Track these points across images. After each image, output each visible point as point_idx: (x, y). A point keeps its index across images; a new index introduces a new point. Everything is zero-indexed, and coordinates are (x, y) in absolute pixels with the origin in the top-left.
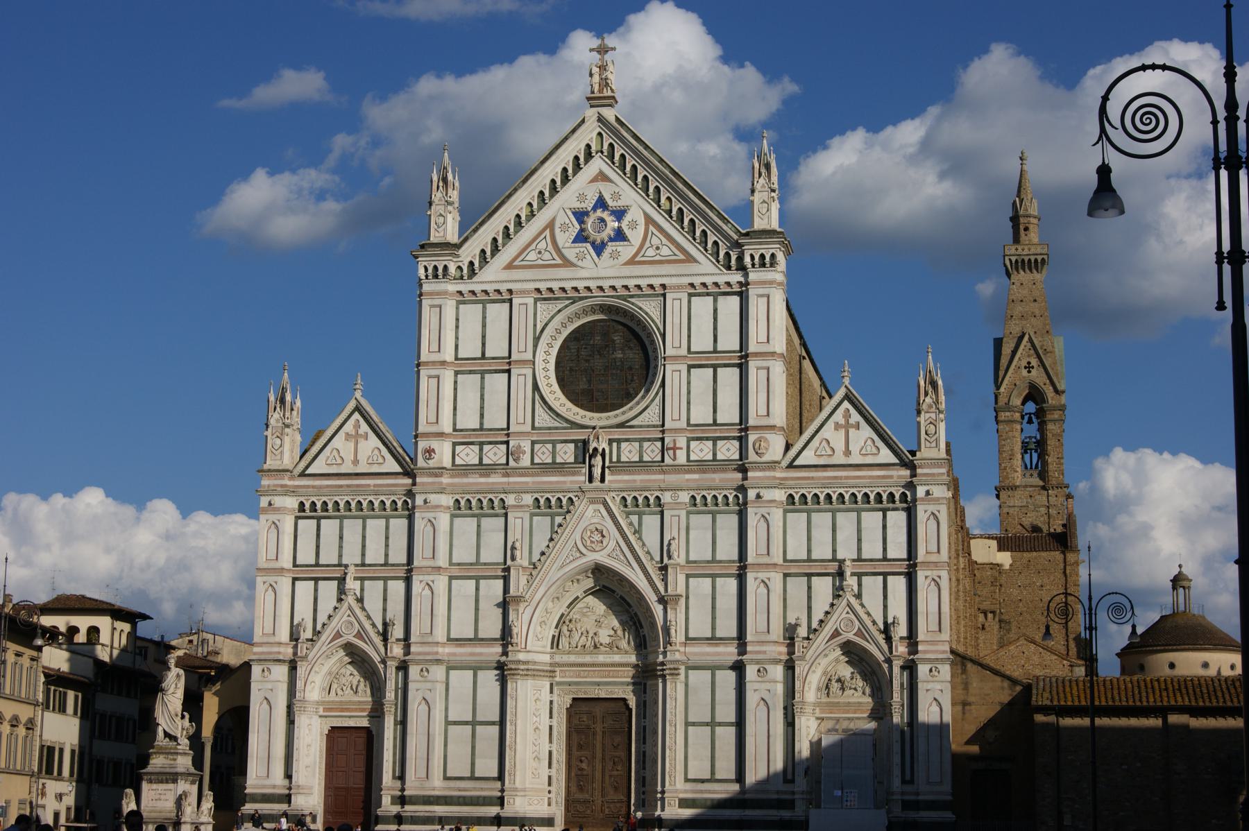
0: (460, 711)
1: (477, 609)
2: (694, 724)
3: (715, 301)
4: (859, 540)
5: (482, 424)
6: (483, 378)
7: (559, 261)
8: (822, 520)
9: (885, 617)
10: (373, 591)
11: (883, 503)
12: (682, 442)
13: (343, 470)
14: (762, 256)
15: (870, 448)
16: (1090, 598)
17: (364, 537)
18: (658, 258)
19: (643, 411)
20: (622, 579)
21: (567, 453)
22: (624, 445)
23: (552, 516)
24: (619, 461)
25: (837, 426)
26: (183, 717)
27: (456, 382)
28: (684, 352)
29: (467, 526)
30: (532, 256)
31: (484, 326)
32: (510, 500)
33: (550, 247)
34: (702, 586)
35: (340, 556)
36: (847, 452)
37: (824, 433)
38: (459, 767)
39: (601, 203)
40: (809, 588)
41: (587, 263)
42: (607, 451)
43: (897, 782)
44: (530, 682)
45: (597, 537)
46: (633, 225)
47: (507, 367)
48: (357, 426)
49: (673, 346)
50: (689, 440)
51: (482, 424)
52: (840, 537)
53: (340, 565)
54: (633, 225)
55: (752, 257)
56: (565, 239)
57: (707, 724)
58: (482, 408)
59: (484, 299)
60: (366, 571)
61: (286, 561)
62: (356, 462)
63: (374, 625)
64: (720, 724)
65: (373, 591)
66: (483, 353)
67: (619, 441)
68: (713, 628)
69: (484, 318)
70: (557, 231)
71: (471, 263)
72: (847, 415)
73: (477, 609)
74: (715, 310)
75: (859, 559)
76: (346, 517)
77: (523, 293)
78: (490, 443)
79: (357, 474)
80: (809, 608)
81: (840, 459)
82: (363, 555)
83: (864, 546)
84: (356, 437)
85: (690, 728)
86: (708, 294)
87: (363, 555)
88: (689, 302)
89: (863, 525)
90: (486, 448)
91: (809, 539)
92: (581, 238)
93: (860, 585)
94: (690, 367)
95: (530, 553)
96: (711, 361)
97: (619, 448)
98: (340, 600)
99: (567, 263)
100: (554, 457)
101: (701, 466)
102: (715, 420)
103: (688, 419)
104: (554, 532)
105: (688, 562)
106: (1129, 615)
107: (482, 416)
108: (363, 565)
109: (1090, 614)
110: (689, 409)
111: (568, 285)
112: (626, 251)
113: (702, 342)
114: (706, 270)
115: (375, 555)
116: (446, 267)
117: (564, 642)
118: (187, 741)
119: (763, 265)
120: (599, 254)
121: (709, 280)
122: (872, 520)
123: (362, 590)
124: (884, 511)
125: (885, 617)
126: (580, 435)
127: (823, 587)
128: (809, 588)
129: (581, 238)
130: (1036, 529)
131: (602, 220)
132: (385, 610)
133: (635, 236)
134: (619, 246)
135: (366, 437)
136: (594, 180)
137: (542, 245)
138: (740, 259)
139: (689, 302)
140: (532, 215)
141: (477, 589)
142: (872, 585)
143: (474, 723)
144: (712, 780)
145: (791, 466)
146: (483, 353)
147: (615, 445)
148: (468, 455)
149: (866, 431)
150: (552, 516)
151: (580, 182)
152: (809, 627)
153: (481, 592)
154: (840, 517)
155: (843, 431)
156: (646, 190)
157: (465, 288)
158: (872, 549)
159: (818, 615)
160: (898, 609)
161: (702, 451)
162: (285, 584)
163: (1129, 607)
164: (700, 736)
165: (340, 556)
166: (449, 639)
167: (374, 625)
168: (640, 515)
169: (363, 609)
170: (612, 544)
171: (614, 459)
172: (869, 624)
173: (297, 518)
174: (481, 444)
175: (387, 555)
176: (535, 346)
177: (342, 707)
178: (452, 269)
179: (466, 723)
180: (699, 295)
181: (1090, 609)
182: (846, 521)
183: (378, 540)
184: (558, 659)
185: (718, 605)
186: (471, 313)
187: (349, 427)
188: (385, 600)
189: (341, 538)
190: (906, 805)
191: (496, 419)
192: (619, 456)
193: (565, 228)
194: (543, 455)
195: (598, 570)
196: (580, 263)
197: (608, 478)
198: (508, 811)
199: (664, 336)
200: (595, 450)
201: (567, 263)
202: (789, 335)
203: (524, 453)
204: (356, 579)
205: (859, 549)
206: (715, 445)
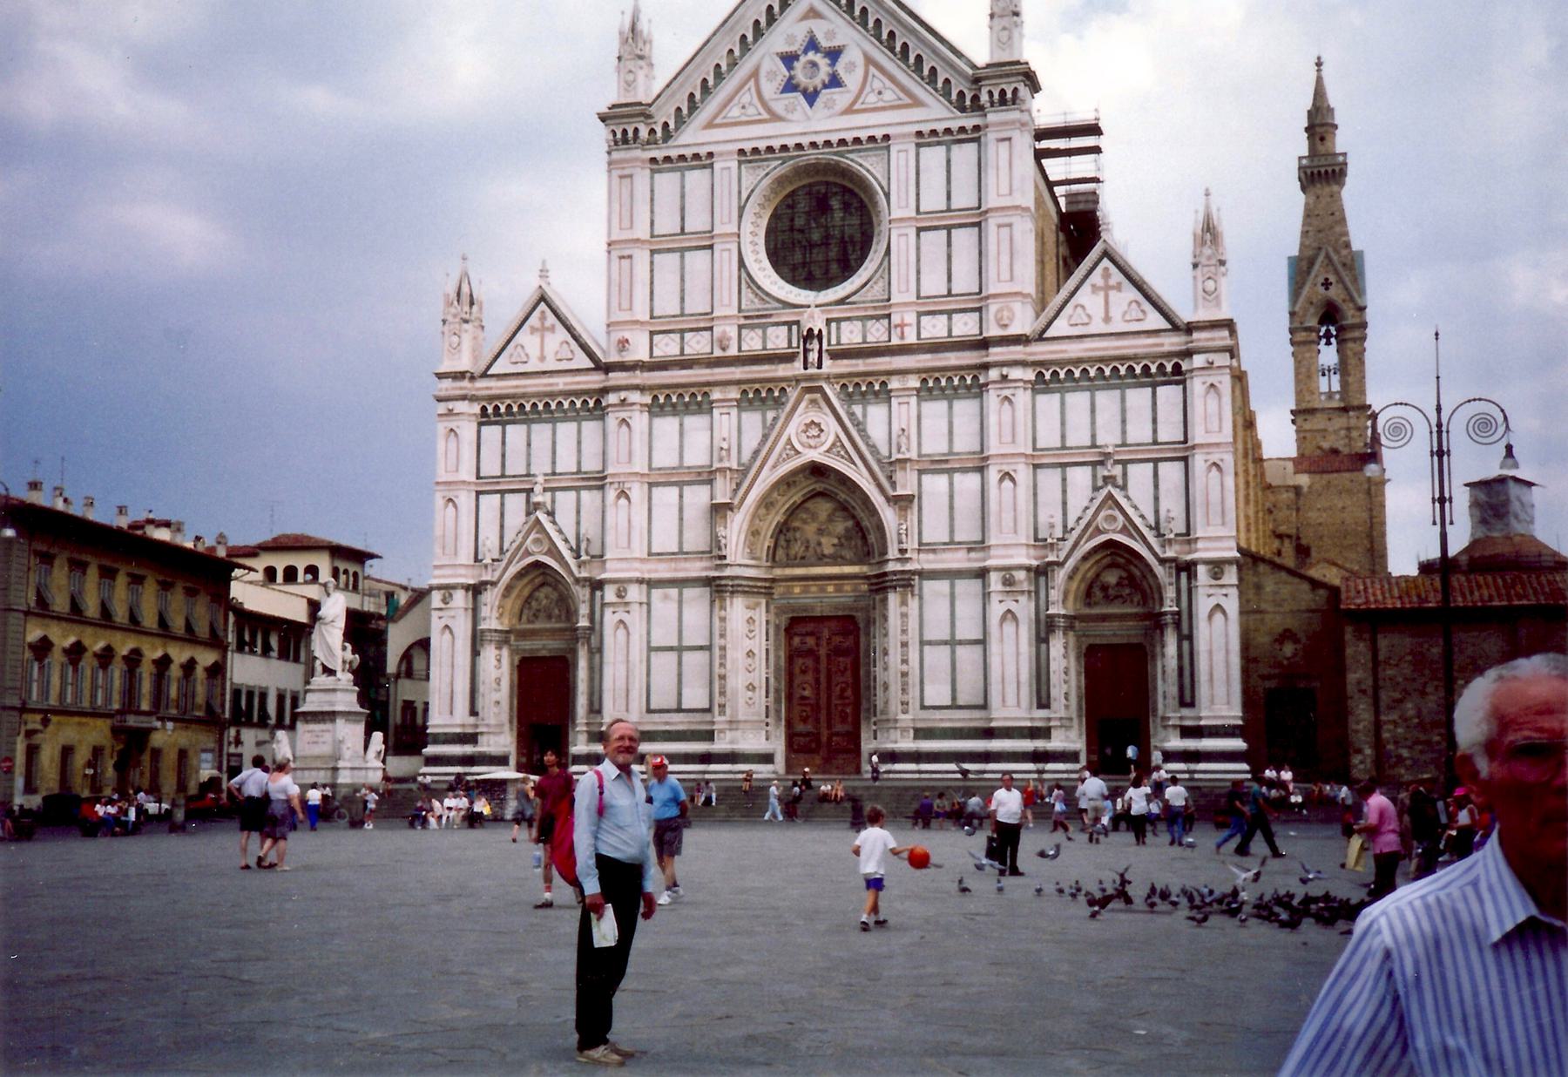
1: (681, 519)
2: (930, 643)
3: (949, 150)
4: (1124, 421)
5: (682, 308)
6: (682, 257)
7: (765, 116)
9: (1157, 512)
10: (566, 501)
12: (911, 318)
14: (1003, 92)
15: (1136, 314)
16: (1439, 409)
17: (554, 443)
18: (880, 104)
20: (844, 480)
22: (844, 325)
24: (838, 343)
25: (1095, 288)
26: (344, 648)
27: (652, 263)
30: (734, 112)
31: (683, 196)
33: (756, 101)
34: (936, 485)
35: (529, 465)
36: (1107, 319)
37: (1080, 297)
38: (663, 697)
39: (812, 45)
40: (1064, 480)
41: (796, 116)
42: (825, 333)
45: (815, 432)
46: (851, 67)
48: (543, 317)
50: (920, 314)
51: (682, 308)
53: (528, 475)
55: (991, 93)
56: (770, 88)
57: (945, 643)
58: (682, 291)
61: (467, 474)
62: (542, 358)
63: (566, 541)
64: (961, 643)
65: (566, 501)
66: (683, 229)
67: (838, 320)
68: (952, 531)
69: (683, 187)
70: (763, 81)
71: (666, 125)
73: (681, 519)
74: (949, 162)
76: (533, 421)
78: (692, 330)
79: (544, 373)
80: (1064, 503)
81: (1098, 326)
82: (554, 463)
83: (1129, 428)
84: (543, 330)
85: (927, 648)
86: (939, 143)
87: (554, 463)
88: (918, 155)
89: (1128, 404)
90: (688, 336)
91: (1063, 423)
92: (790, 86)
93: (1125, 474)
94: (919, 230)
95: (739, 452)
96: (946, 223)
97: (838, 328)
100: (764, 342)
101: (936, 347)
102: (949, 291)
103: (918, 291)
105: (920, 455)
106: (1502, 429)
107: (682, 299)
108: (554, 474)
109: (1440, 432)
110: (918, 280)
112: (840, 98)
114: (937, 113)
115: (566, 463)
116: (636, 130)
117: (780, 553)
118: (351, 676)
120: (811, 104)
121: (940, 127)
122: (1138, 398)
123: (553, 501)
125: (1157, 512)
128: (1064, 480)
129: (790, 86)
130: (1335, 452)
131: (814, 64)
132: (578, 523)
133: (852, 80)
136: (805, 17)
137: (746, 99)
138: (976, 98)
139: (918, 155)
140: (733, 64)
141: (681, 496)
143: (680, 649)
146: (683, 229)
147: (834, 325)
149: (1132, 293)
152: (1065, 526)
153: (685, 499)
155: (1102, 294)
156: (864, 24)
160: (1172, 505)
161: (935, 328)
162: (465, 499)
163: (1500, 418)
165: (529, 465)
166: (650, 554)
167: (566, 541)
169: (554, 523)
170: (831, 439)
171: (834, 341)
172: (1138, 521)
173: (480, 424)
174: (682, 332)
175: (579, 463)
176: (740, 217)
177: (533, 634)
178: (644, 133)
179: (671, 649)
180: (929, 145)
181: (1439, 425)
182: (1107, 400)
184: (778, 572)
185: (956, 505)
186: (667, 182)
187: (534, 320)
188: (578, 512)
189: (529, 445)
192: (838, 338)
193: (772, 75)
194: (753, 343)
195: (817, 470)
196: (789, 116)
197: (827, 362)
198: (719, 746)
199: (887, 195)
200: (810, 330)
201: (775, 117)
202: (1036, 187)
203: (729, 339)
204: (545, 490)
205: (1124, 432)
206: (950, 319)
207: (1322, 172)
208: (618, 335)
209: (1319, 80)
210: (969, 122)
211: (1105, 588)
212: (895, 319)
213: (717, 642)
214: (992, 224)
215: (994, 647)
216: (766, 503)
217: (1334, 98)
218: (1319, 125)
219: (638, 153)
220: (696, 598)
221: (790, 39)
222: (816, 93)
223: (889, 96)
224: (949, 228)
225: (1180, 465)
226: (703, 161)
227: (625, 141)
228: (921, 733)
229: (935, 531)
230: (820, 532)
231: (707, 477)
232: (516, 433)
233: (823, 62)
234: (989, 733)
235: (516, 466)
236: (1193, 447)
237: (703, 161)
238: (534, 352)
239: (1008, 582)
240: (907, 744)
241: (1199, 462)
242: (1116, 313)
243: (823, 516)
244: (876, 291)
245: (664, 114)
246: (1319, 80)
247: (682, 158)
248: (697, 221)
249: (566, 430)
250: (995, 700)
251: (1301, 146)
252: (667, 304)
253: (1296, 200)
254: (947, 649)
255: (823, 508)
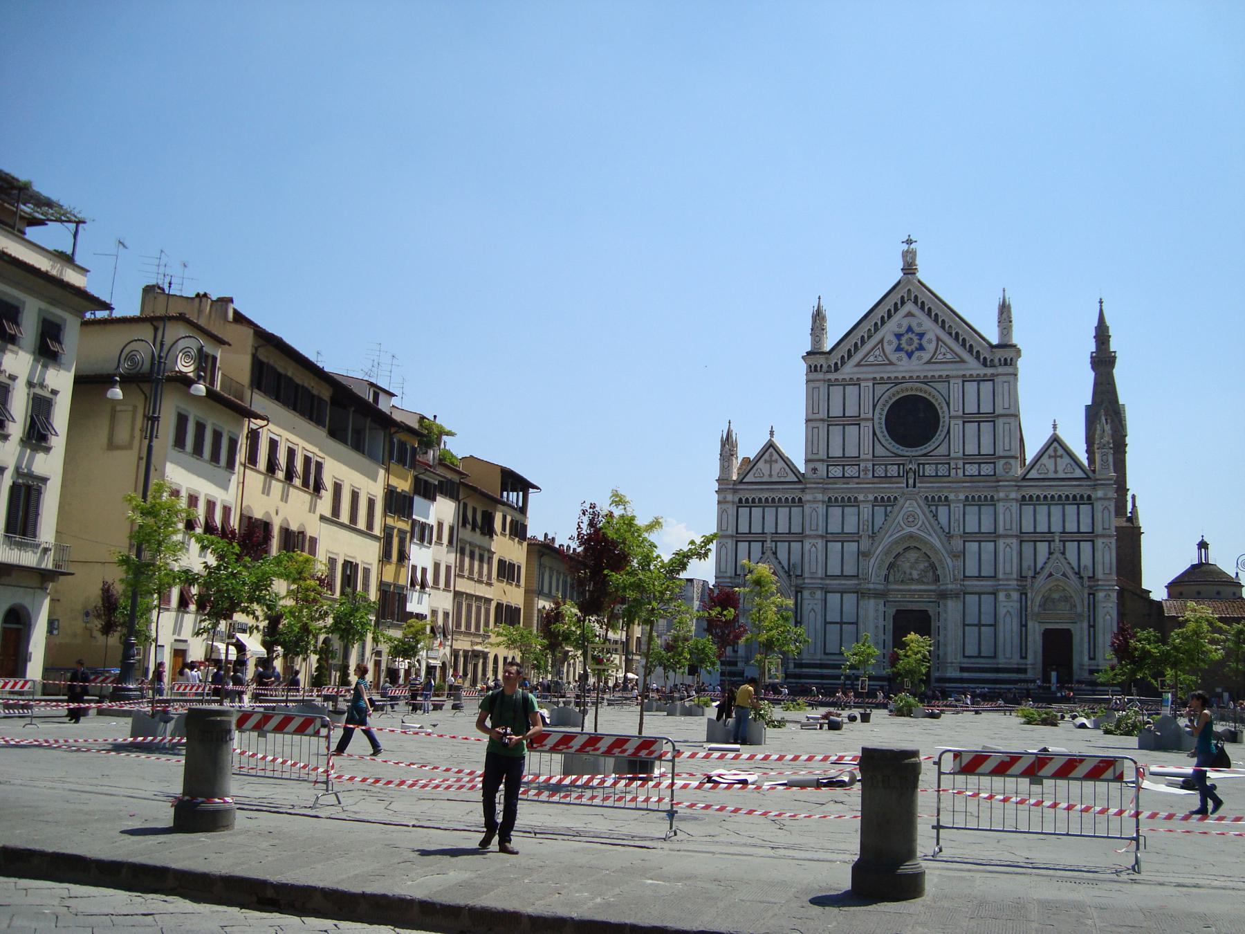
0: (833, 616)
4: (1064, 522)
8: (1042, 510)
10: (782, 548)
11: (1077, 501)
12: (960, 464)
13: (764, 480)
15: (1069, 469)
19: (937, 446)
20: (925, 542)
21: (893, 470)
23: (886, 507)
28: (960, 413)
29: (836, 512)
30: (871, 359)
32: (861, 497)
34: (973, 547)
36: (1056, 472)
39: (910, 329)
43: (1086, 658)
44: (872, 602)
46: (930, 341)
47: (857, 421)
48: (771, 455)
49: (955, 408)
52: (1052, 519)
54: (930, 341)
56: (889, 349)
59: (844, 384)
60: (777, 537)
62: (770, 476)
72: (1055, 450)
75: (1064, 532)
77: (867, 380)
81: (1052, 475)
84: (771, 462)
98: (763, 553)
99: (891, 363)
104: (886, 515)
111: (893, 375)
113: (971, 408)
114: (973, 367)
115: (783, 528)
117: (891, 578)
119: (1006, 364)
121: (975, 373)
122: (1071, 510)
124: (1078, 505)
126: (899, 460)
127: (1043, 548)
133: (931, 347)
134: (922, 353)
135: (776, 461)
137: (877, 353)
140: (869, 337)
142: (1071, 547)
143: (841, 623)
144: (979, 656)
145: (1024, 479)
148: (836, 472)
149: (1067, 460)
150: (886, 507)
151: (897, 318)
154: (1052, 508)
157: (830, 376)
158: (1071, 527)
159: (1039, 566)
161: (972, 470)
164: (972, 632)
168: (937, 506)
178: (825, 366)
182: (1056, 511)
183: (782, 520)
186: (836, 392)
187: (766, 456)
190: (1091, 672)
191: (852, 451)
193: (890, 342)
194: (880, 471)
195: (911, 536)
199: (948, 404)
201: (891, 363)
207: (1103, 361)
208: (811, 465)
209: (1101, 311)
210: (989, 371)
211: (1053, 601)
212: (953, 466)
213: (861, 620)
214: (1000, 422)
215: (1001, 628)
216: (888, 552)
217: (1108, 322)
218: (1102, 335)
219: (820, 376)
220: (850, 599)
221: (900, 326)
222: (912, 352)
223: (949, 356)
224: (979, 422)
225: (1089, 544)
226: (856, 383)
227: (816, 370)
228: (962, 669)
229: (972, 570)
230: (911, 568)
231: (855, 537)
232: (757, 512)
233: (916, 339)
234: (998, 670)
235: (756, 528)
236: (1097, 536)
237: (856, 383)
238: (767, 473)
239: (1008, 596)
240: (957, 674)
241: (1099, 542)
242: (1060, 469)
243: (912, 560)
244: (942, 450)
245: (835, 358)
246: (1101, 311)
247: (844, 379)
248: (851, 411)
249: (783, 512)
250: (1000, 655)
251: (1092, 346)
252: (836, 452)
253: (1090, 376)
254: (976, 629)
255: (912, 556)
